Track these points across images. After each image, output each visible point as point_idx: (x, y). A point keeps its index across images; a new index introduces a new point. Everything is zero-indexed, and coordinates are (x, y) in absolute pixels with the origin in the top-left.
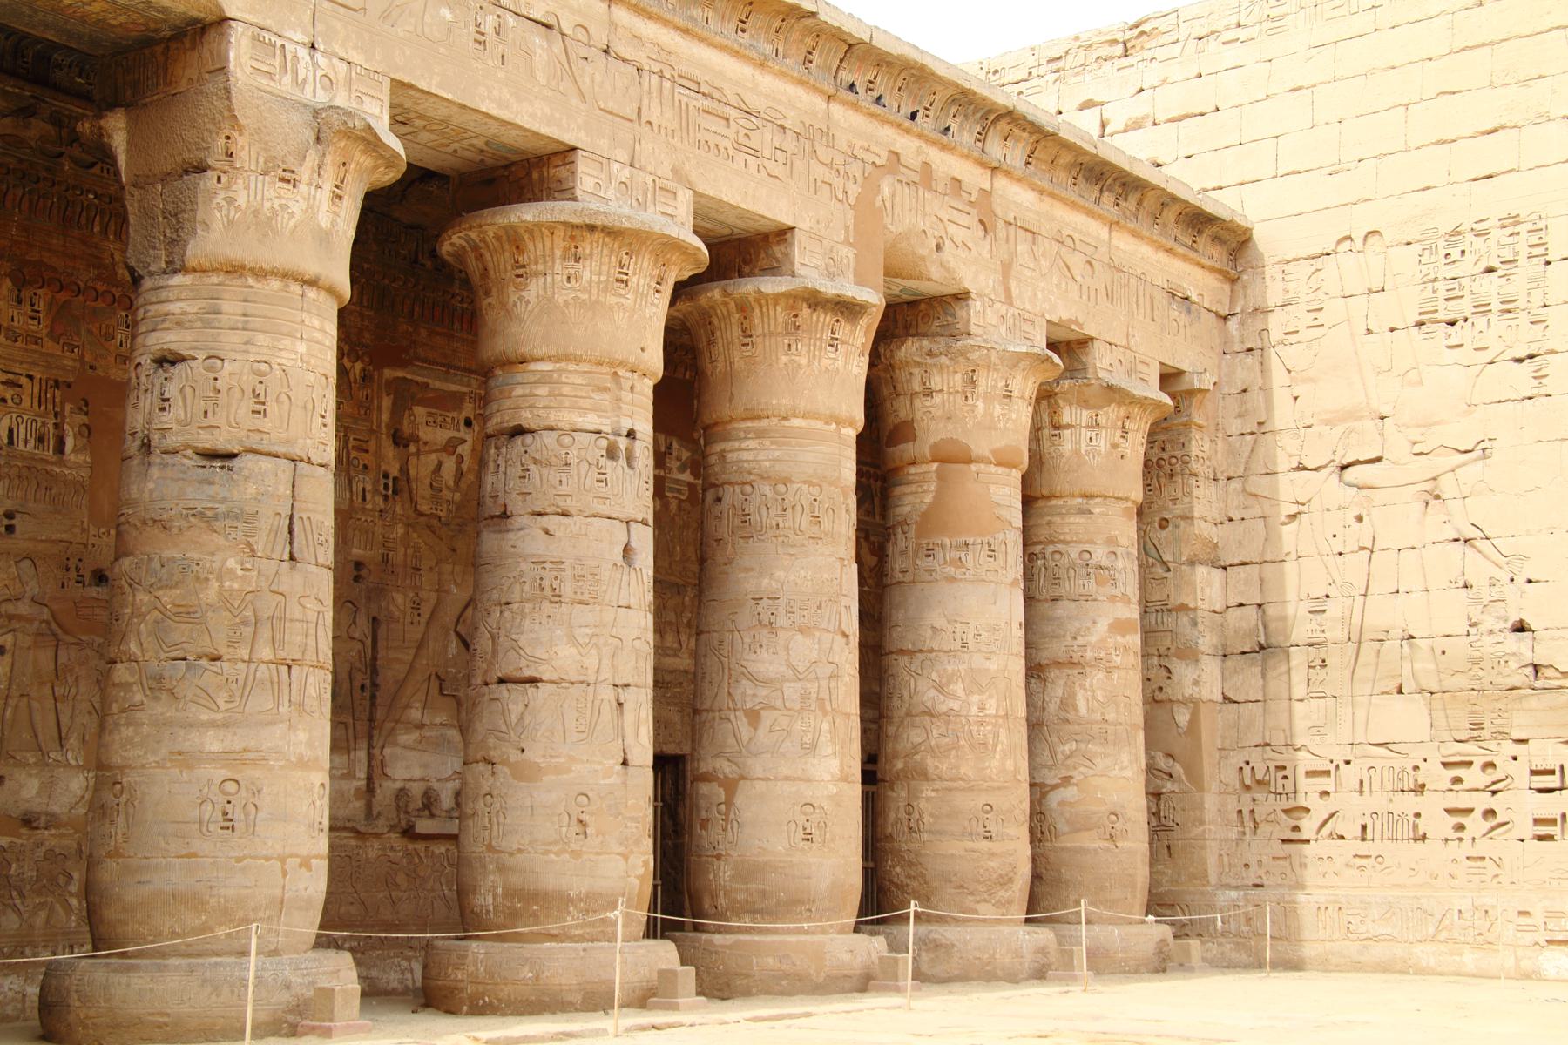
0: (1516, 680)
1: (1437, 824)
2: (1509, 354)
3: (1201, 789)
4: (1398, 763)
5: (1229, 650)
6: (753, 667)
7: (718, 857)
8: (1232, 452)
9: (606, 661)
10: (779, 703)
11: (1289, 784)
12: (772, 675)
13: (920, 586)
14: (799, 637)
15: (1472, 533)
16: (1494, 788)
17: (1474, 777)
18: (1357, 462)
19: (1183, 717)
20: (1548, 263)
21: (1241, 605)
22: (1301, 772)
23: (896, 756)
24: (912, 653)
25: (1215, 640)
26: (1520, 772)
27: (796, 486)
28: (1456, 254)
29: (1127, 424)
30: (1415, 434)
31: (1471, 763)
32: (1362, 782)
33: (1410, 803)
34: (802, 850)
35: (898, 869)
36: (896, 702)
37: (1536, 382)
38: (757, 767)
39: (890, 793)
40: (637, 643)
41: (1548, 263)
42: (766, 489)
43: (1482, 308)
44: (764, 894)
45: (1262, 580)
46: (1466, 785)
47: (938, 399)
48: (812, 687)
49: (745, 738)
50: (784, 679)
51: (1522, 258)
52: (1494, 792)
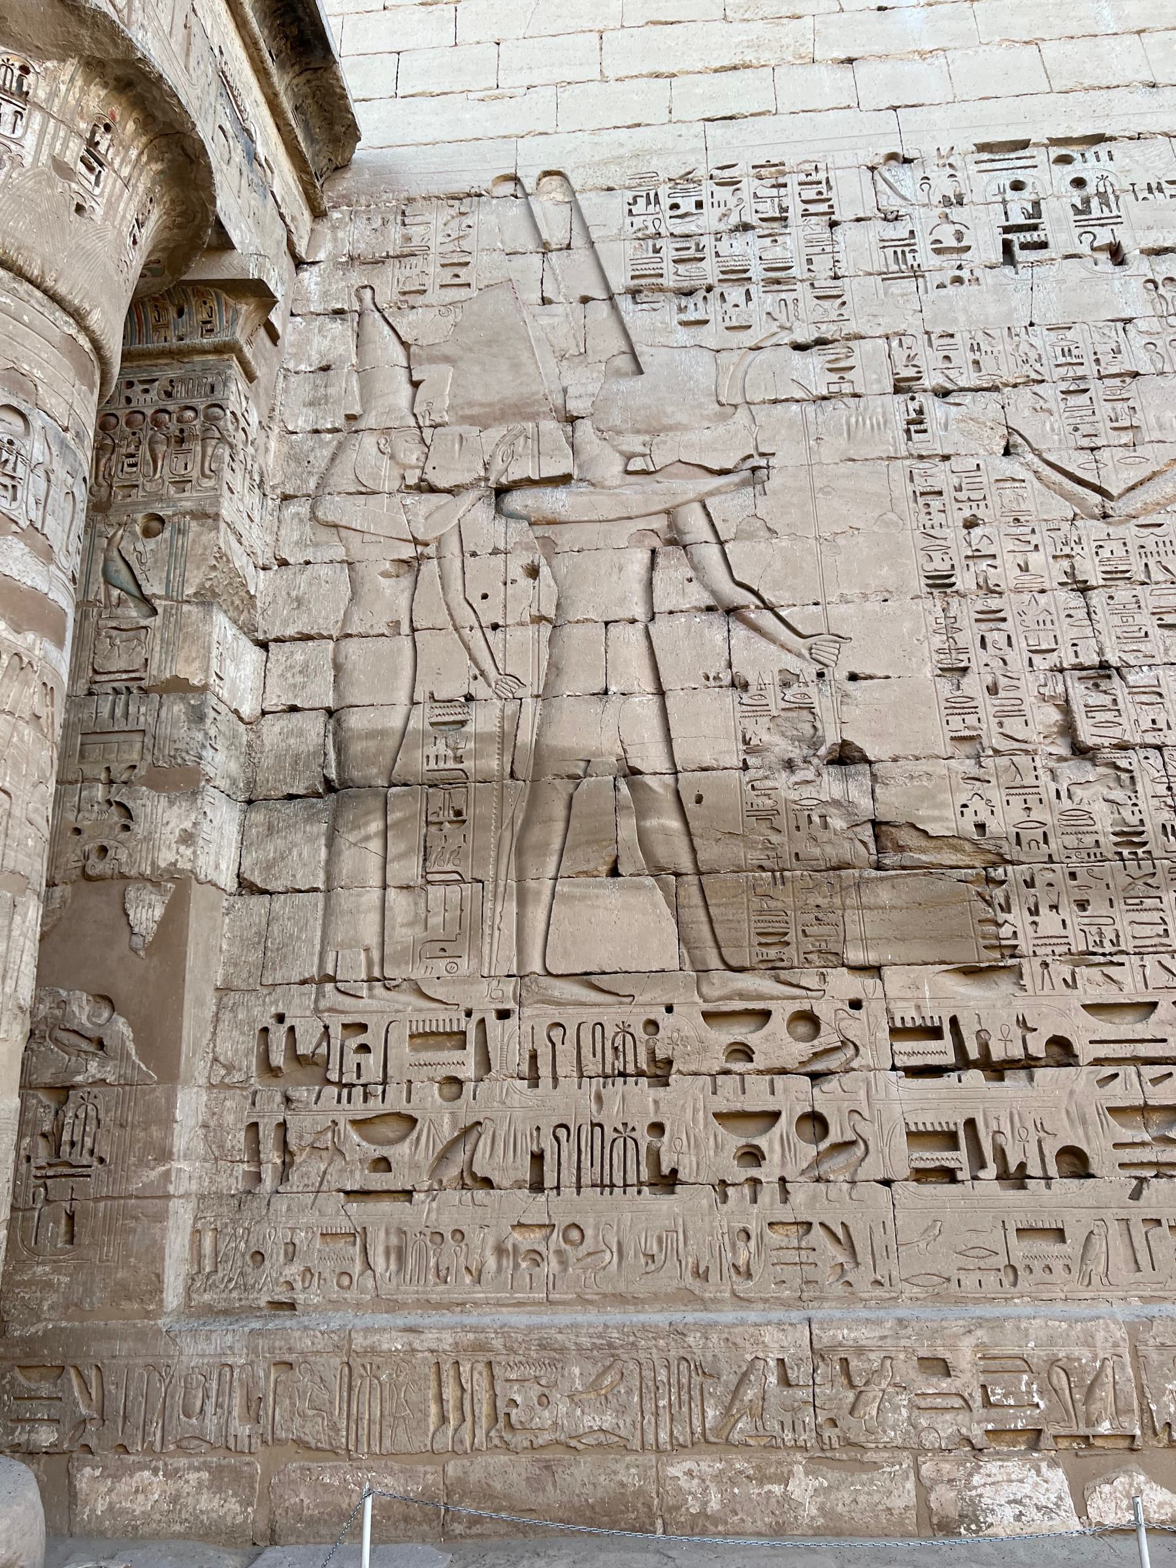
0: (846, 851)
3: (170, 1073)
4: (612, 1015)
5: (261, 792)
8: (295, 457)
11: (372, 1062)
15: (742, 597)
16: (818, 1066)
17: (777, 1043)
18: (530, 482)
19: (147, 913)
20: (833, 224)
21: (293, 709)
22: (400, 1034)
25: (234, 767)
26: (870, 1030)
28: (687, 205)
29: (104, 141)
30: (634, 443)
31: (766, 1015)
32: (534, 1057)
37: (835, 377)
43: (738, 276)
45: (337, 667)
46: (759, 1062)
51: (794, 214)
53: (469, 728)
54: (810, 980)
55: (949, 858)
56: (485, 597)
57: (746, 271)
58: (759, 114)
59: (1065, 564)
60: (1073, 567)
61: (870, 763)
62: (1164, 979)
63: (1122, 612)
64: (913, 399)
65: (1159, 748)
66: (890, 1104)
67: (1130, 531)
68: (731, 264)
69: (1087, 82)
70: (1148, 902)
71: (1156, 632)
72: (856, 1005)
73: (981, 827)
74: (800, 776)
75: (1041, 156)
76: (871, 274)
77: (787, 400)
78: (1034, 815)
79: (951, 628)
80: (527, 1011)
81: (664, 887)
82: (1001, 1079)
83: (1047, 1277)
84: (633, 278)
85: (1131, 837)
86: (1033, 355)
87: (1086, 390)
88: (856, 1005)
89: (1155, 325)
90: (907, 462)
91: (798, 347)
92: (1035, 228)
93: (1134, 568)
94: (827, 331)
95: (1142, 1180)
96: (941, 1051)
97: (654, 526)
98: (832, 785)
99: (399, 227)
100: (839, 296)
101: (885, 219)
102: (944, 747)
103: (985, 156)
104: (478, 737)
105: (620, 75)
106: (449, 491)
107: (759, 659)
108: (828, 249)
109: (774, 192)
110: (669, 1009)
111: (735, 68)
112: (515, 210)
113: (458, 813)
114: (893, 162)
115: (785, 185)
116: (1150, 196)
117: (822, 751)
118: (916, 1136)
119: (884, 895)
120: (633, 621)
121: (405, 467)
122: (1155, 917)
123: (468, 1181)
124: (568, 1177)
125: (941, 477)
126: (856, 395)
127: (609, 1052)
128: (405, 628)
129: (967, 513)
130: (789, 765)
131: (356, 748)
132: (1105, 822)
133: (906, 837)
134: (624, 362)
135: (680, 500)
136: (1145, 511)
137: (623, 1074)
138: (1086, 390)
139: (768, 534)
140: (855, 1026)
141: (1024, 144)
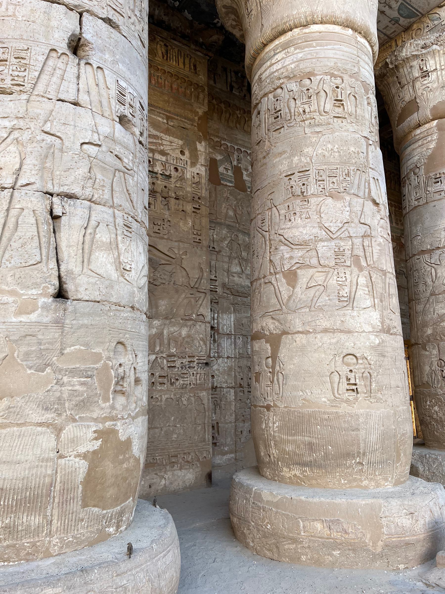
6: (288, 234)
7: (268, 408)
9: (30, 161)
10: (314, 261)
12: (307, 237)
13: (432, 204)
14: (330, 200)
23: (425, 325)
24: (430, 252)
27: (319, 77)
34: (347, 401)
35: (436, 408)
36: (421, 287)
38: (297, 323)
39: (424, 352)
40: (92, 150)
42: (293, 86)
44: (311, 447)
47: (433, 76)
48: (346, 245)
49: (285, 296)
50: (317, 239)
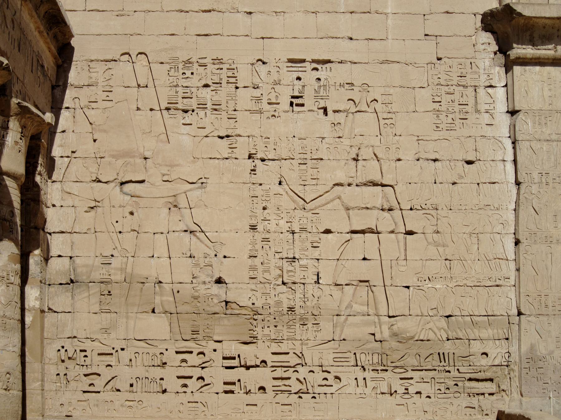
0: (217, 309)
1: (173, 384)
2: (216, 133)
4: (152, 350)
16: (203, 365)
17: (193, 359)
20: (237, 88)
21: (60, 256)
28: (188, 74)
32: (131, 360)
33: (158, 372)
37: (230, 150)
41: (237, 88)
43: (202, 106)
51: (224, 82)
52: (203, 368)
53: (112, 266)
54: (203, 343)
55: (243, 311)
56: (117, 222)
57: (206, 104)
58: (216, 35)
59: (289, 224)
60: (291, 225)
61: (226, 284)
62: (293, 346)
63: (302, 242)
64: (253, 162)
65: (304, 284)
66: (217, 375)
67: (309, 215)
68: (202, 101)
69: (330, 35)
70: (292, 327)
71: (310, 249)
72: (215, 350)
73: (253, 304)
74: (207, 286)
75: (309, 66)
76: (246, 110)
77: (214, 158)
78: (268, 302)
79: (254, 243)
80: (129, 349)
81: (167, 317)
82: (249, 369)
83: (252, 414)
84: (168, 103)
85: (291, 309)
86: (292, 149)
87: (306, 164)
88: (215, 350)
89: (331, 141)
90: (249, 185)
91: (221, 138)
92: (301, 97)
93: (308, 227)
94: (229, 132)
95: (277, 394)
96: (235, 363)
97: (170, 201)
98: (216, 289)
99: (88, 73)
100: (235, 118)
101: (254, 88)
102: (247, 280)
103: (290, 64)
104: (116, 269)
105: (168, 10)
106: (106, 183)
107: (198, 247)
108: (234, 98)
109: (218, 71)
110: (167, 350)
111: (210, 11)
112: (129, 66)
113: (109, 292)
114: (260, 62)
115: (222, 69)
116: (340, 89)
117: (214, 280)
118: (225, 383)
119: (226, 322)
120: (162, 233)
121: (92, 173)
122: (293, 330)
123: (114, 390)
124: (139, 390)
125: (259, 191)
126: (236, 158)
127: (150, 360)
128: (93, 231)
129: (264, 205)
130: (204, 283)
131: (79, 270)
132: (285, 305)
133: (234, 306)
134: (164, 137)
135: (179, 192)
136: (316, 208)
137: (153, 366)
138: (306, 164)
139: (204, 207)
140: (213, 355)
141: (304, 61)
